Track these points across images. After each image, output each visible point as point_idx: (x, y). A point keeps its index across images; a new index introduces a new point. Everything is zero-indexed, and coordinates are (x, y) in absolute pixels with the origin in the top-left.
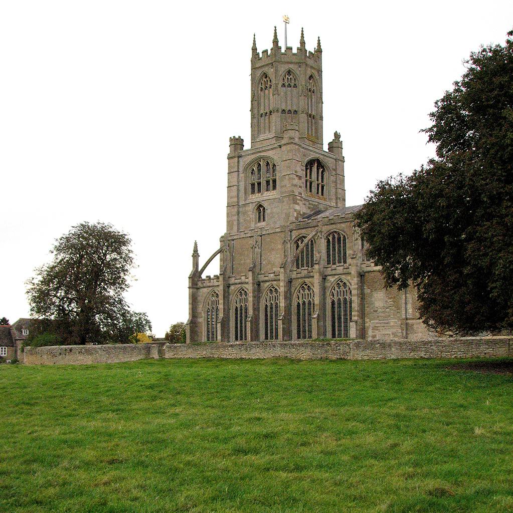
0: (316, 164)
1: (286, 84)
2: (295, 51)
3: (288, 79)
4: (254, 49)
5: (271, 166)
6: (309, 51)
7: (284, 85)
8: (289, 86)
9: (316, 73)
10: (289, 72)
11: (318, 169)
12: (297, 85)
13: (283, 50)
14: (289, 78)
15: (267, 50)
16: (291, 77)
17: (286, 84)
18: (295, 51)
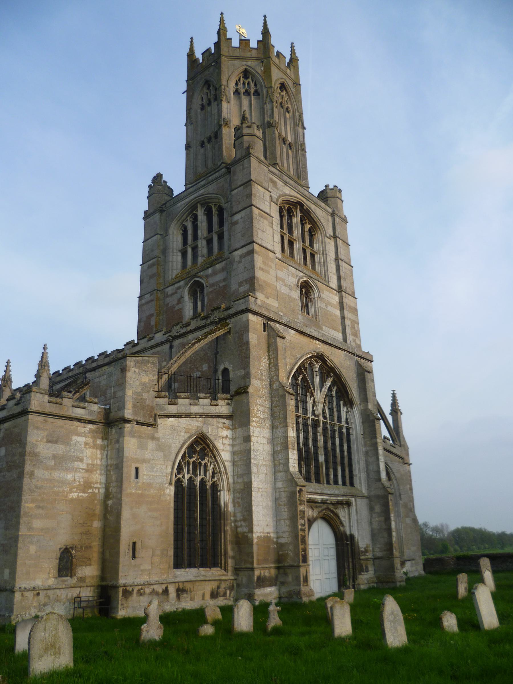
0: (299, 215)
1: (242, 91)
2: (254, 44)
3: (244, 83)
4: (191, 55)
5: (215, 212)
6: (277, 51)
7: (237, 92)
8: (247, 93)
9: (290, 83)
10: (246, 74)
11: (303, 225)
12: (260, 90)
13: (236, 43)
14: (246, 82)
15: (210, 48)
16: (249, 80)
17: (242, 91)
18: (254, 44)
